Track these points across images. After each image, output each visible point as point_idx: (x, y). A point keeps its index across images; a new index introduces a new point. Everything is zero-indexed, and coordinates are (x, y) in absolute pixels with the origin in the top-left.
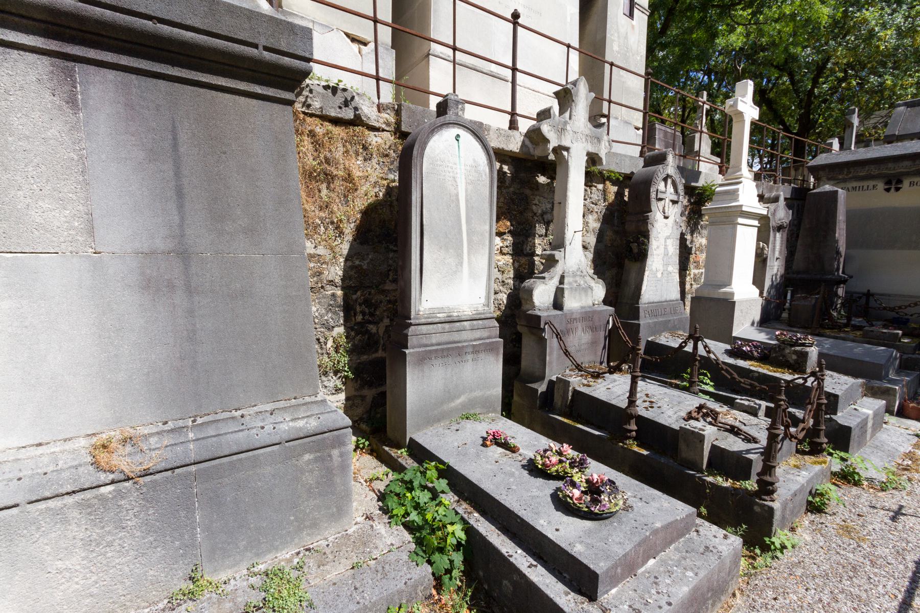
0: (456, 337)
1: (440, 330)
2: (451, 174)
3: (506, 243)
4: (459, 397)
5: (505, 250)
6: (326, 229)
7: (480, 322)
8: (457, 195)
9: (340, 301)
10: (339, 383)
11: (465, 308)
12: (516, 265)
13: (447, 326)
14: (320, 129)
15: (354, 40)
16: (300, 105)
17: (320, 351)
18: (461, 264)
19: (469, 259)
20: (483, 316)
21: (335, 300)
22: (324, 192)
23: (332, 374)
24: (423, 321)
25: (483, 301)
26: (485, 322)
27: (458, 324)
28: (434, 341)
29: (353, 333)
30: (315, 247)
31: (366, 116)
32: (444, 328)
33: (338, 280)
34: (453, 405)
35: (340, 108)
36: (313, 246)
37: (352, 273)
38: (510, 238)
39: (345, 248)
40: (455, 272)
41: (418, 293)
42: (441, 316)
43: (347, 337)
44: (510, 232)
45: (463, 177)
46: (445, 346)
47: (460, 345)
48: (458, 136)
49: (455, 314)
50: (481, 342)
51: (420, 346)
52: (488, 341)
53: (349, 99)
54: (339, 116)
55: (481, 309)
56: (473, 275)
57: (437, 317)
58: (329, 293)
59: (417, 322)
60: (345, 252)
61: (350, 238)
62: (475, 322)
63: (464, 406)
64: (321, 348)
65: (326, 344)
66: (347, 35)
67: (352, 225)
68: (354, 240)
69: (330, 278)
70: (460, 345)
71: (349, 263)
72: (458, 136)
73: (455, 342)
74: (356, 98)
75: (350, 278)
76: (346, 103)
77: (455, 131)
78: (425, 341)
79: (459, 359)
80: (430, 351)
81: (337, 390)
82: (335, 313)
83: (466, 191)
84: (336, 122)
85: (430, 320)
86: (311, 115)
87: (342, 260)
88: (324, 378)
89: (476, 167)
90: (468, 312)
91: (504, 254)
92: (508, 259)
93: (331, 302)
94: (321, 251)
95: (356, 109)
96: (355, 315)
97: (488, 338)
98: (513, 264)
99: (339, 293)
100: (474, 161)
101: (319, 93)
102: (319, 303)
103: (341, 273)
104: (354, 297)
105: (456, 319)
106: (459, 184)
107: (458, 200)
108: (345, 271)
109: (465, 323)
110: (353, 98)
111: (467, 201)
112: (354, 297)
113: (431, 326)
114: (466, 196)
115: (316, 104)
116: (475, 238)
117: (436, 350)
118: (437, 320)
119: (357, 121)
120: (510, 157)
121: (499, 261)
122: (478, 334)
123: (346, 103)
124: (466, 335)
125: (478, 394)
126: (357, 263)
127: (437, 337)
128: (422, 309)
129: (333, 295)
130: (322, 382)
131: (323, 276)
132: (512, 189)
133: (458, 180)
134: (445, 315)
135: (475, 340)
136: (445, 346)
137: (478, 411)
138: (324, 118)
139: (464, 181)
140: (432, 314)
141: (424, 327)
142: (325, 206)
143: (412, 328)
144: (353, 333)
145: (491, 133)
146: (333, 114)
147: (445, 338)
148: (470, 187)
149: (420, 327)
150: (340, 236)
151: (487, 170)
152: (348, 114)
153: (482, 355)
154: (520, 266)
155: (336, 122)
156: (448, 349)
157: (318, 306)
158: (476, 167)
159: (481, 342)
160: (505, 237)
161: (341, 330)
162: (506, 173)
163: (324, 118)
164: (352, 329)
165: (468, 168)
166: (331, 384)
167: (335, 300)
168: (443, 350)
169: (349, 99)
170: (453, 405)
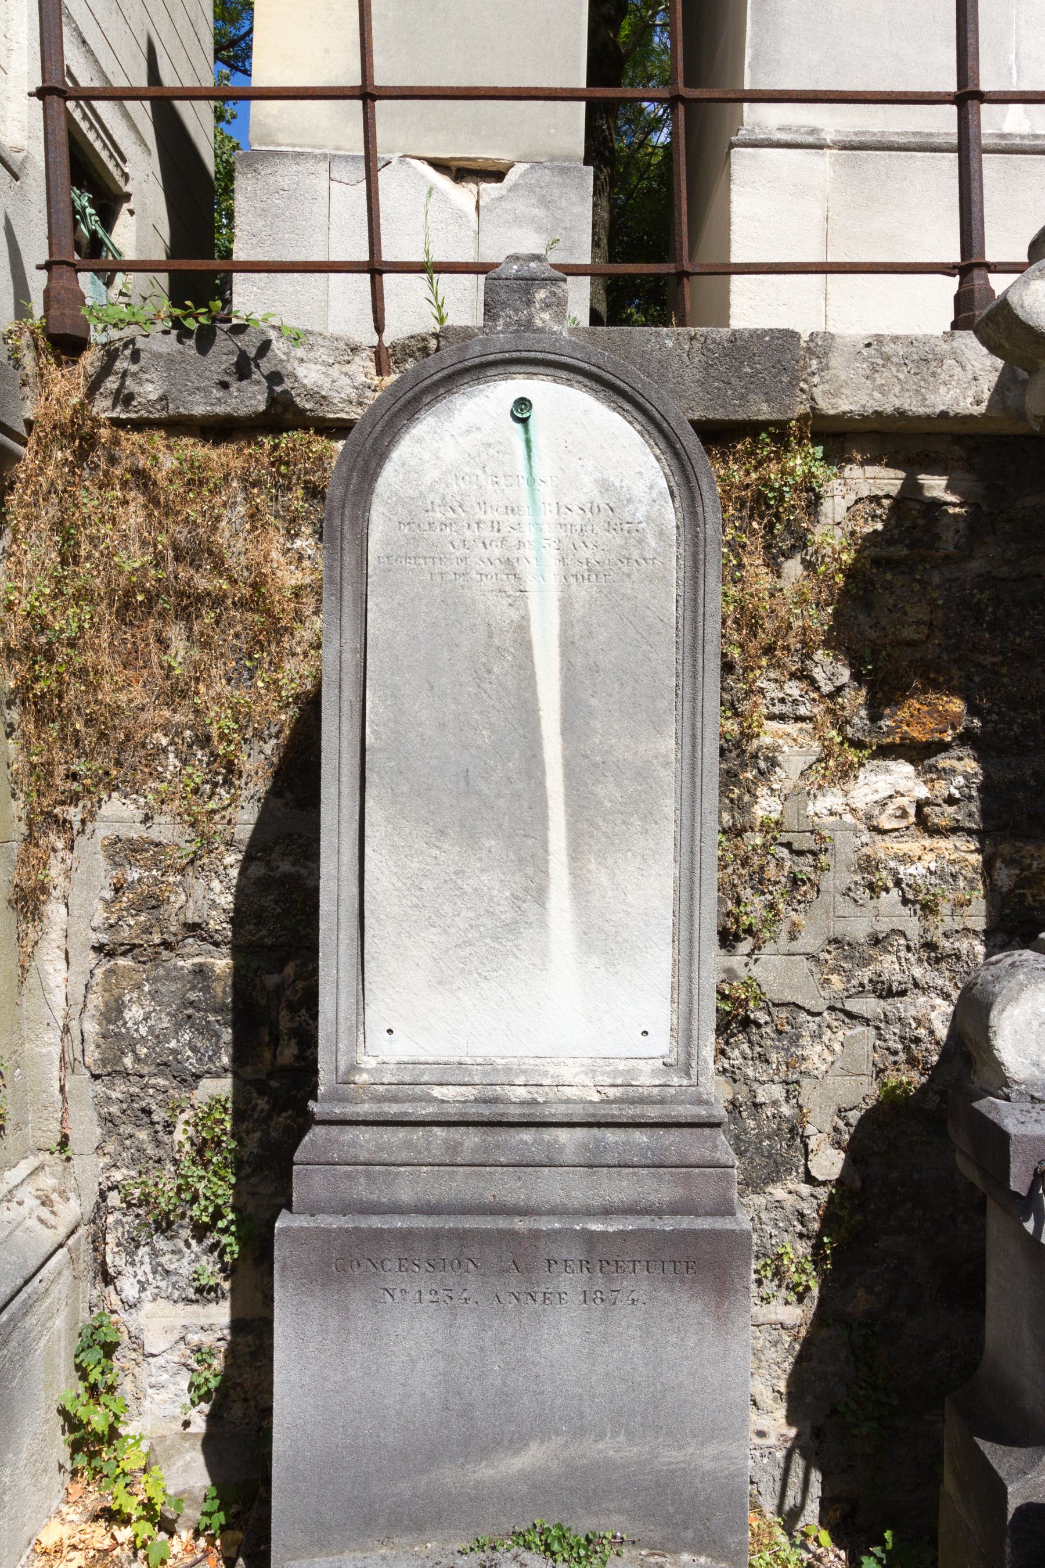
0: (508, 1187)
1: (437, 1153)
2: (496, 552)
3: (954, 787)
4: (517, 1443)
5: (942, 815)
6: (185, 762)
7: (641, 1137)
8: (522, 628)
9: (222, 991)
10: (209, 1268)
11: (567, 1074)
12: (1004, 876)
13: (471, 1139)
14: (168, 457)
15: (461, 172)
16: (109, 403)
17: (150, 1150)
18: (540, 894)
19: (577, 873)
20: (653, 1113)
21: (206, 989)
22: (179, 646)
23: (185, 1233)
24: (365, 1109)
25: (661, 1045)
26: (672, 1137)
27: (527, 1136)
28: (405, 1195)
29: (263, 1104)
30: (147, 819)
31: (311, 395)
32: (454, 1148)
33: (218, 923)
34: (485, 1472)
35: (224, 385)
36: (140, 815)
37: (268, 901)
38: (971, 766)
39: (245, 820)
40: (512, 927)
41: (347, 1001)
42: (451, 1096)
43: (238, 1117)
44: (966, 738)
45: (551, 556)
46: (450, 1223)
47: (520, 1224)
48: (523, 403)
49: (522, 1093)
50: (630, 1224)
51: (347, 1208)
52: (668, 1224)
53: (252, 353)
54: (220, 410)
55: (647, 1079)
56: (598, 937)
57: (432, 1100)
58: (188, 964)
59: (338, 1110)
60: (244, 832)
61: (260, 786)
62: (611, 1136)
63: (540, 1488)
64: (158, 1144)
65: (169, 1127)
66: (439, 165)
67: (269, 748)
68: (274, 792)
69: (191, 917)
70: (520, 1224)
71: (257, 870)
72: (523, 403)
73: (524, 1212)
74: (279, 347)
75: (260, 919)
76: (243, 369)
77: (506, 390)
78: (362, 1190)
79: (514, 1280)
80: (378, 1234)
81: (205, 1293)
82: (205, 1030)
83: (566, 605)
84: (218, 430)
85: (392, 1110)
86: (139, 425)
87: (232, 858)
88: (161, 1243)
89: (611, 508)
90: (580, 1086)
91: (934, 831)
92: (965, 852)
93: (193, 996)
94: (165, 829)
95: (275, 378)
96: (275, 1040)
97: (676, 1210)
98: (988, 868)
99: (222, 963)
100: (606, 487)
101: (158, 356)
102: (154, 994)
103: (226, 900)
104: (271, 980)
105: (514, 1113)
106: (531, 584)
107: (525, 646)
108: (241, 893)
109: (563, 1135)
110: (265, 347)
111: (567, 645)
112: (271, 980)
113: (401, 1134)
114: (566, 626)
115: (149, 390)
116: (607, 791)
117: (406, 1236)
118: (426, 1111)
119: (283, 414)
120: (958, 438)
121: (905, 859)
122: (620, 1188)
123: (243, 369)
124: (554, 1187)
125: (611, 1449)
126: (285, 867)
127: (419, 1179)
128: (368, 1062)
129: (200, 971)
130: (155, 1253)
131: (169, 911)
132: (976, 565)
133: (528, 570)
134: (470, 1092)
135: (607, 1212)
136: (450, 1223)
137: (613, 1524)
138: (178, 426)
139: (553, 566)
140: (413, 1080)
141: (365, 1135)
142: (176, 693)
143: (316, 1134)
144: (263, 1104)
145: (836, 361)
146: (199, 410)
147: (457, 1185)
148: (582, 593)
149: (351, 1134)
150: (227, 782)
151: (670, 515)
152: (250, 399)
153: (636, 1285)
154: (1021, 883)
155: (218, 430)
156: (462, 1236)
157: (149, 1005)
158: (611, 508)
159: (630, 1224)
160: (943, 761)
161: (223, 1087)
162: (938, 504)
163: (178, 426)
164: (262, 1089)
165: (575, 518)
166: (184, 1267)
167: (206, 989)
168: (436, 1236)
169: (252, 353)
170: (485, 1472)
